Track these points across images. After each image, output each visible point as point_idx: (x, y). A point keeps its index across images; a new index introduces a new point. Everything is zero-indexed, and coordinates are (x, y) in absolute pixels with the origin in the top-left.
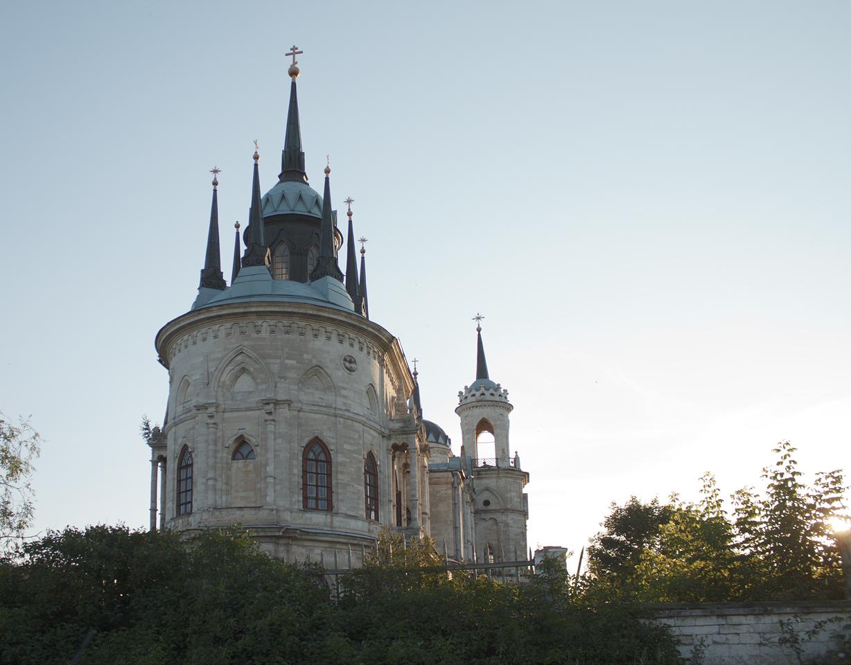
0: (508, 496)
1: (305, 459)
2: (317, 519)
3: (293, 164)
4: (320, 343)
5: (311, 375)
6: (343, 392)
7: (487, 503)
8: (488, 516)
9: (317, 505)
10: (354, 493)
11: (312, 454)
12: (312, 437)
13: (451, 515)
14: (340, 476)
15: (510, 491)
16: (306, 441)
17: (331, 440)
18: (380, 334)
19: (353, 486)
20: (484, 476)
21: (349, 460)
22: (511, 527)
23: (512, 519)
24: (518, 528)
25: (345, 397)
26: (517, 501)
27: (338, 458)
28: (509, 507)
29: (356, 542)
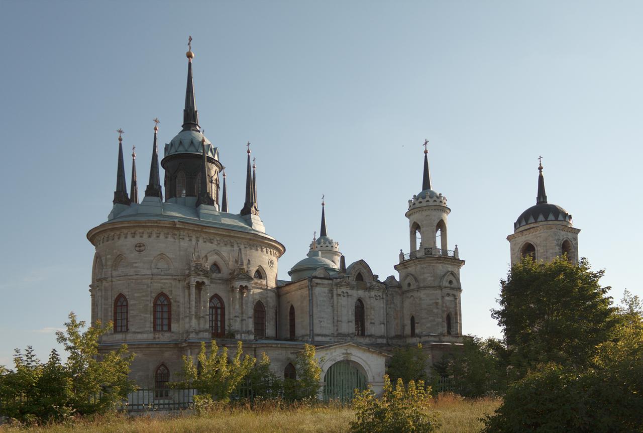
4: (122, 241)
5: (119, 260)
6: (134, 265)
7: (409, 285)
8: (409, 295)
9: (162, 328)
11: (160, 302)
12: (118, 294)
13: (308, 307)
14: (131, 312)
16: (115, 297)
17: (127, 293)
20: (408, 266)
21: (137, 302)
25: (137, 267)
27: (131, 302)
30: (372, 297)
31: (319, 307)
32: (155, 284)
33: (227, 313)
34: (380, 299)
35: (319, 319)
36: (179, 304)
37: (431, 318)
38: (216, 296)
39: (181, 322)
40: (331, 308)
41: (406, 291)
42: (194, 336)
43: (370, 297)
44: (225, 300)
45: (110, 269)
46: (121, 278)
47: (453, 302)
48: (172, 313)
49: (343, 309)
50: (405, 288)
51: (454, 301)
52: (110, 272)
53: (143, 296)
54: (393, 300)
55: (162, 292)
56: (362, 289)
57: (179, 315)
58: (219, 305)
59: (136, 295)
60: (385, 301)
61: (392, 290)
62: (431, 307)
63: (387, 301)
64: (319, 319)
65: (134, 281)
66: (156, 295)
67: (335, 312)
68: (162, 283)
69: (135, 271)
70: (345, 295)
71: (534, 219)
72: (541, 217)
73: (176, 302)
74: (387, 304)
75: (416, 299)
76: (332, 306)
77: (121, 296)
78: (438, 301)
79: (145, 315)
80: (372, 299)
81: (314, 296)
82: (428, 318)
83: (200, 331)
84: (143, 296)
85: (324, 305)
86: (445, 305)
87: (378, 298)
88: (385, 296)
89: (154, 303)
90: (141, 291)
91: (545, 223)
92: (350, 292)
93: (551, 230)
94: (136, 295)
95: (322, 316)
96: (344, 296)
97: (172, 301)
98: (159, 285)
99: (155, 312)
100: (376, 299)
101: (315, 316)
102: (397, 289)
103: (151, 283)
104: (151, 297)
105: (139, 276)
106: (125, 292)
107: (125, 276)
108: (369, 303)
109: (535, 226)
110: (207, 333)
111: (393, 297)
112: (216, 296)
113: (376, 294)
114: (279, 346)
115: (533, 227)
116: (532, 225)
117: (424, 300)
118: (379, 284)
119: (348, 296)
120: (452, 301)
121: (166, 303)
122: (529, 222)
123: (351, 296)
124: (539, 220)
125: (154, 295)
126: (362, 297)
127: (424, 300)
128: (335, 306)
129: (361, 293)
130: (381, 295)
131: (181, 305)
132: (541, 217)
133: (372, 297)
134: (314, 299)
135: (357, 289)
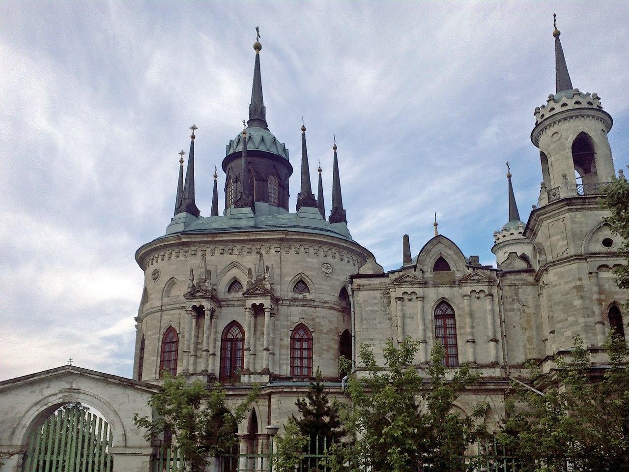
22: (556, 285)
24: (566, 283)
31: (364, 322)
32: (165, 317)
34: (485, 296)
37: (571, 319)
38: (234, 324)
49: (408, 321)
54: (517, 296)
60: (496, 299)
63: (501, 298)
68: (171, 315)
70: (414, 297)
76: (390, 319)
80: (465, 298)
82: (567, 319)
85: (375, 319)
87: (482, 295)
88: (495, 291)
92: (420, 291)
98: (169, 317)
100: (478, 298)
102: (524, 276)
112: (234, 324)
114: (295, 390)
119: (417, 298)
123: (423, 297)
129: (445, 292)
130: (485, 289)
135: (436, 286)
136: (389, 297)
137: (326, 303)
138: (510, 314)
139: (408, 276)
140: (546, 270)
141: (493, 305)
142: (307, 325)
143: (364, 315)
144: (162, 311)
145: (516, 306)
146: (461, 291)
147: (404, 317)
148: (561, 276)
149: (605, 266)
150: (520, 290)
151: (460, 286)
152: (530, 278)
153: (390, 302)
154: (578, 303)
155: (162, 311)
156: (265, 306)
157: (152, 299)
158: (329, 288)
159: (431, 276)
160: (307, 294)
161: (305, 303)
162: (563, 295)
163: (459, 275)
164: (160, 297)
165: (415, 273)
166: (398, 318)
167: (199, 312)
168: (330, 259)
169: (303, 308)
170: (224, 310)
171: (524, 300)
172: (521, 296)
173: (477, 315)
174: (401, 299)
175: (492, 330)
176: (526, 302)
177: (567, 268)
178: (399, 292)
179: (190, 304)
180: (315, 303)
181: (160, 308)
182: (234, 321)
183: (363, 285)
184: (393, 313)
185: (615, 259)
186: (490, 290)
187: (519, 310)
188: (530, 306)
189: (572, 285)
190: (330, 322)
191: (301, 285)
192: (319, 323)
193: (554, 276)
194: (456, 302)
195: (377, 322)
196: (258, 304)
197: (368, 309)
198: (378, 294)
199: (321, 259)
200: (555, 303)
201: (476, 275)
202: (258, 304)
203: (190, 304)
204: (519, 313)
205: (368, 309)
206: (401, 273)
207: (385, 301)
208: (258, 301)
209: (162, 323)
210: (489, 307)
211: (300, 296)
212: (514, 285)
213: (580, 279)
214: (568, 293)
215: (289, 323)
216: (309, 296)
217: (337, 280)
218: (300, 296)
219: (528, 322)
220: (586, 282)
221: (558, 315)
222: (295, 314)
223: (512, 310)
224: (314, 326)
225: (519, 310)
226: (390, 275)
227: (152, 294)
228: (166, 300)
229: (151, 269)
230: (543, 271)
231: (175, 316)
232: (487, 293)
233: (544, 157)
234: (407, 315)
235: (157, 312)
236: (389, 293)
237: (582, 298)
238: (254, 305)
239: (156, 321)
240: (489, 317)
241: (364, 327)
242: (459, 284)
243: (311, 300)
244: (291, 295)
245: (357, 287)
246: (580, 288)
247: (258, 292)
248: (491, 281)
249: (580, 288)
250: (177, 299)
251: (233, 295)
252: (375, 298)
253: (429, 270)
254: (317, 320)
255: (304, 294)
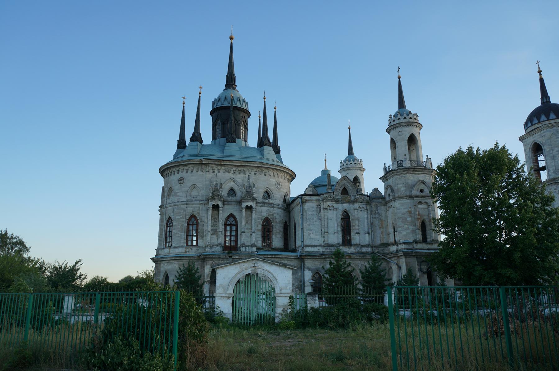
0: (396, 188)
1: (167, 227)
2: (166, 251)
3: (231, 82)
5: (171, 192)
8: (389, 205)
10: (178, 237)
15: (397, 184)
18: (192, 162)
19: (179, 234)
23: (399, 204)
24: (404, 209)
26: (403, 190)
27: (174, 223)
28: (397, 195)
29: (173, 259)
30: (356, 209)
31: (308, 220)
32: (189, 208)
33: (239, 229)
35: (309, 232)
36: (204, 223)
38: (231, 215)
39: (204, 238)
40: (319, 221)
41: (388, 201)
42: (209, 250)
43: (355, 209)
44: (238, 218)
45: (166, 199)
46: (170, 205)
47: (426, 210)
48: (199, 231)
49: (329, 221)
50: (387, 199)
51: (428, 208)
52: (165, 201)
53: (181, 218)
55: (193, 215)
56: (347, 202)
57: (203, 232)
58: (234, 223)
59: (177, 217)
60: (369, 212)
61: (376, 201)
62: (405, 215)
63: (371, 211)
64: (309, 232)
65: (176, 206)
66: (189, 217)
67: (323, 225)
69: (177, 199)
70: (332, 208)
71: (538, 120)
72: (543, 118)
73: (201, 222)
74: (371, 214)
75: (394, 209)
76: (321, 219)
77: (170, 218)
78: (410, 210)
79: (182, 233)
80: (356, 210)
81: (304, 211)
83: (213, 246)
84: (181, 218)
85: (313, 219)
86: (417, 213)
87: (363, 209)
88: (368, 207)
89: (187, 223)
90: (180, 214)
91: (548, 122)
92: (336, 205)
93: (553, 129)
94: (177, 217)
95: (311, 229)
96: (330, 210)
97: (199, 221)
98: (192, 209)
99: (188, 230)
100: (361, 211)
101: (305, 229)
102: (381, 200)
103: (186, 207)
104: (186, 219)
105: (179, 203)
106: (172, 217)
107: (173, 203)
108: (354, 214)
109: (539, 125)
110: (219, 247)
111: (377, 207)
112: (231, 215)
113: (360, 205)
115: (538, 127)
116: (537, 126)
117: (399, 209)
118: (363, 196)
119: (334, 209)
120: (426, 208)
121: (195, 223)
122: (534, 123)
123: (337, 209)
124: (541, 120)
125: (188, 217)
126: (347, 209)
127: (399, 209)
128: (322, 219)
129: (346, 206)
130: (364, 206)
131: (205, 225)
132: (543, 118)
133: (356, 209)
134: (304, 214)
135: (342, 203)
136: (320, 208)
137: (278, 205)
138: (374, 219)
139: (330, 197)
140: (394, 200)
141: (367, 215)
142: (270, 218)
143: (308, 217)
144: (187, 204)
145: (377, 216)
146: (353, 207)
147: (328, 219)
148: (402, 205)
149: (420, 203)
150: (379, 208)
151: (353, 204)
152: (383, 202)
153: (320, 210)
154: (409, 219)
155: (187, 204)
156: (253, 207)
157: (178, 196)
158: (280, 197)
159: (340, 198)
160: (270, 200)
161: (270, 205)
162: (402, 214)
163: (353, 198)
164: (185, 195)
165: (333, 195)
166: (325, 219)
167: (216, 208)
168: (280, 180)
169: (268, 208)
170: (226, 207)
171: (380, 213)
172: (379, 211)
173: (360, 220)
174: (326, 209)
175: (367, 228)
176: (381, 214)
177: (405, 201)
178: (326, 206)
179: (211, 204)
180: (275, 206)
181: (186, 203)
182: (231, 214)
183: (308, 200)
184: (322, 216)
185: (424, 199)
186: (366, 207)
187: (378, 218)
188: (383, 216)
189: (407, 210)
190: (280, 216)
191: (268, 195)
192: (276, 217)
193: (399, 204)
194: (352, 212)
195: (314, 221)
196: (249, 206)
197: (310, 213)
198: (315, 205)
199: (276, 180)
200: (399, 218)
201: (361, 198)
202: (249, 206)
203: (211, 203)
204: (378, 220)
205: (310, 213)
206: (327, 195)
207: (318, 209)
208: (249, 204)
209: (187, 212)
210: (366, 216)
211: (267, 201)
212: (377, 205)
213: (410, 208)
214: (404, 214)
215: (261, 217)
216: (271, 201)
217: (283, 192)
218: (267, 201)
219: (382, 224)
220: (412, 209)
221: (399, 223)
222: (263, 211)
223: (375, 218)
224: (273, 218)
225: (378, 218)
226: (321, 196)
227: (178, 193)
228: (189, 198)
229: (174, 177)
230: (392, 201)
231: (196, 208)
232: (365, 208)
233: (393, 142)
234: (329, 218)
235: (184, 204)
236: (320, 205)
237: (411, 217)
238: (247, 206)
239: (183, 210)
240: (366, 221)
241: (308, 223)
242: (353, 203)
243: (272, 203)
244: (261, 200)
245: (304, 201)
246: (410, 212)
247: (249, 198)
248: (368, 203)
249: (410, 212)
250: (197, 198)
251: (229, 199)
252: (313, 208)
253: (340, 194)
254: (275, 215)
255: (269, 200)
